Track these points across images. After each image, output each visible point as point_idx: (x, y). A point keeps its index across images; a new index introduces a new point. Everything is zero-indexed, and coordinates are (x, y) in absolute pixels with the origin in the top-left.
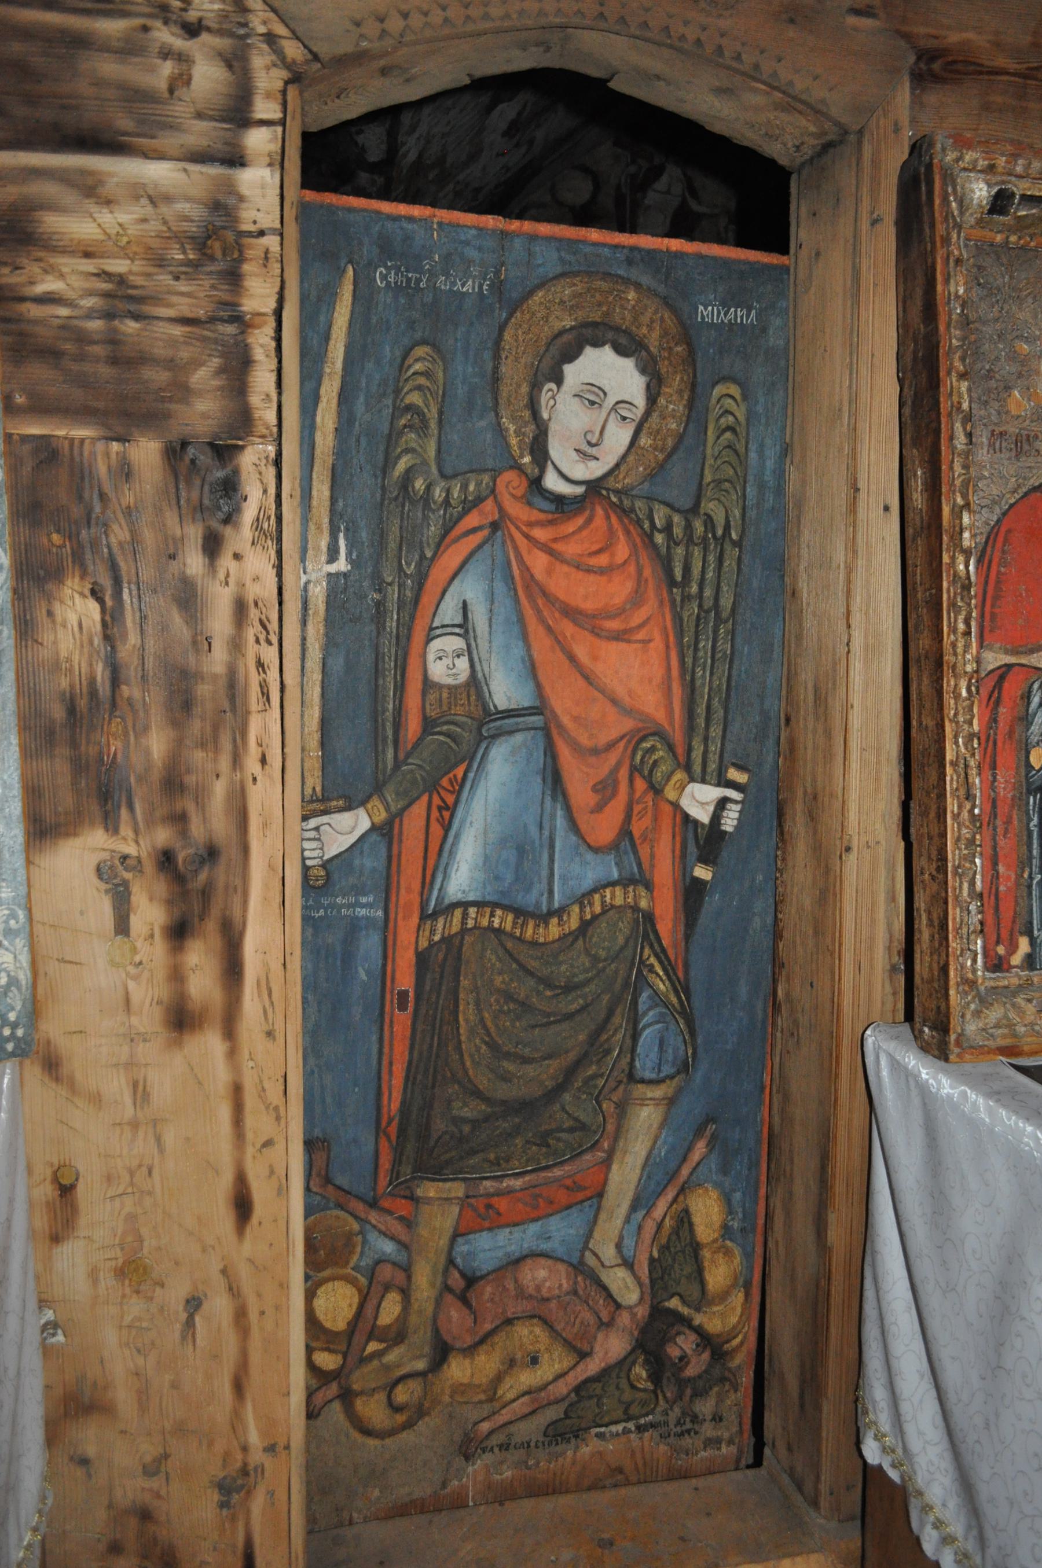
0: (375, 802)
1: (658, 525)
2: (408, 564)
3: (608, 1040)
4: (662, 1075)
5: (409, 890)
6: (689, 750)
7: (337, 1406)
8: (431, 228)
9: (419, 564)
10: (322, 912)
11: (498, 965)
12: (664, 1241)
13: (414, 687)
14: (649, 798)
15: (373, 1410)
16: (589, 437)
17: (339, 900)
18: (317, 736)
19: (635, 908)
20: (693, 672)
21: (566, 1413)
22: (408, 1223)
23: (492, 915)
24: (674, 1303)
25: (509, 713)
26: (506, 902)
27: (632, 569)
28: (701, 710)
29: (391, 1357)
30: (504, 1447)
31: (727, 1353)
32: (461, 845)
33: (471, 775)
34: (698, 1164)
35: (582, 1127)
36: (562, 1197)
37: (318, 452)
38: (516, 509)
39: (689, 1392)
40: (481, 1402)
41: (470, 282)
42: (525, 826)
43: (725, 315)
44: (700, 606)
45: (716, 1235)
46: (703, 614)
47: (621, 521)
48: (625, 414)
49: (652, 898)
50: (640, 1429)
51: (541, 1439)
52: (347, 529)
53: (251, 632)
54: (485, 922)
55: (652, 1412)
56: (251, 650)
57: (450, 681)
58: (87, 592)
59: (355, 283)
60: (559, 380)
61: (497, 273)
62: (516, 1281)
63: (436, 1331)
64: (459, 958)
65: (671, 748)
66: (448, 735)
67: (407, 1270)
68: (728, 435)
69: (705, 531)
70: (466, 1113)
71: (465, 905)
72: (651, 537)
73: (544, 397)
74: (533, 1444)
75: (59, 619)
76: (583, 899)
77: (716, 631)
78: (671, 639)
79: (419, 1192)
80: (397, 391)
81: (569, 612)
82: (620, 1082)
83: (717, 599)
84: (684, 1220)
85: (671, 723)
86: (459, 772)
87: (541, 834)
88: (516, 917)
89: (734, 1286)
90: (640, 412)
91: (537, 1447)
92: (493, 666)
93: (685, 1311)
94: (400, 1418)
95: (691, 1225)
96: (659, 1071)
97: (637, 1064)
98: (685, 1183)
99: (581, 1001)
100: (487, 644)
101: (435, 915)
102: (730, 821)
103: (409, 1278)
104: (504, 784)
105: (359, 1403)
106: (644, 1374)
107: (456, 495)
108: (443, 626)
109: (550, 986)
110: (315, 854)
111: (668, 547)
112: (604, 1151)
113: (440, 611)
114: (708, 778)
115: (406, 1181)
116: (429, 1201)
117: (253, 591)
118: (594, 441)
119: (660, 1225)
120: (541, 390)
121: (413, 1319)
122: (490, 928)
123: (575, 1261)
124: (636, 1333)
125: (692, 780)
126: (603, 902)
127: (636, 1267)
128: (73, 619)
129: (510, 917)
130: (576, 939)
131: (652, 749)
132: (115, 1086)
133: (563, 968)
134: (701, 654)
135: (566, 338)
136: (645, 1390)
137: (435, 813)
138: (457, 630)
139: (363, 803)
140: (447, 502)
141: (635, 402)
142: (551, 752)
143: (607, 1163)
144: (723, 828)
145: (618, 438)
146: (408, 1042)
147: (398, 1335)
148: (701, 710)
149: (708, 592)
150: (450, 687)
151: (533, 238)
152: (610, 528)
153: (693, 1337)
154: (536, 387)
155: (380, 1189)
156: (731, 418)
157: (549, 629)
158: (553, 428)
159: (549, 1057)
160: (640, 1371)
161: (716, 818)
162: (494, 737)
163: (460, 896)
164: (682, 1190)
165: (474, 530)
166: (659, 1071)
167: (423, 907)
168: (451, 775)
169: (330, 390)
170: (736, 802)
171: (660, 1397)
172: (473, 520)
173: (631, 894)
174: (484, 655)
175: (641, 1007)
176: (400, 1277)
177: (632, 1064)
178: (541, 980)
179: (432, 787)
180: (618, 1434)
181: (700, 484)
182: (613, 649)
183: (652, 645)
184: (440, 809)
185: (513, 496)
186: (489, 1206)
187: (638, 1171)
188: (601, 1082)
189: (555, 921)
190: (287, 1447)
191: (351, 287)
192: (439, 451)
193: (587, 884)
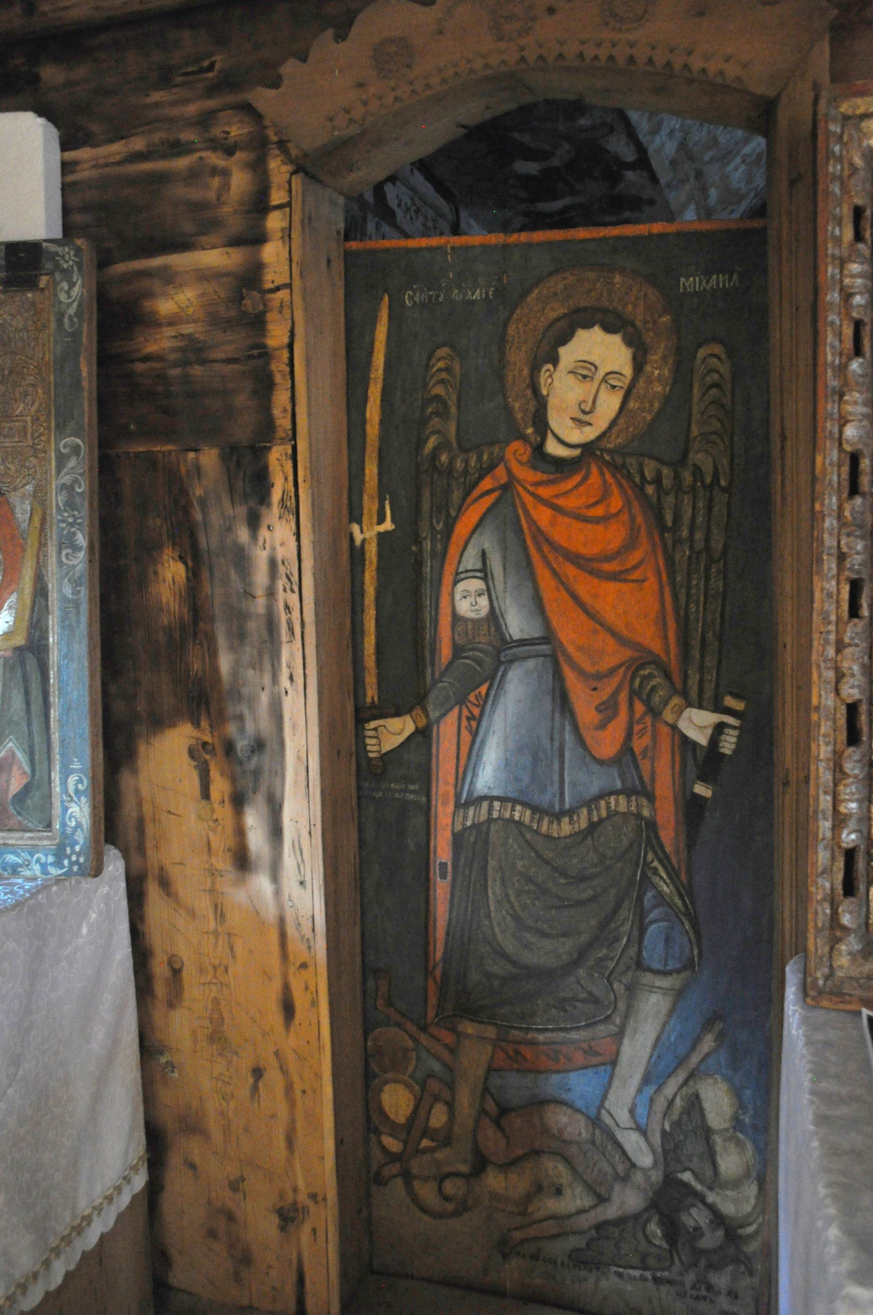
0: (418, 711)
1: (649, 479)
2: (438, 523)
3: (616, 929)
4: (668, 968)
5: (446, 783)
6: (686, 678)
7: (399, 1183)
8: (446, 254)
9: (445, 524)
10: (381, 794)
11: (519, 851)
12: (675, 1117)
13: (445, 622)
14: (648, 720)
15: (427, 1192)
16: (583, 407)
17: (393, 785)
18: (373, 658)
19: (638, 816)
20: (687, 606)
21: (588, 1244)
22: (452, 1051)
23: (513, 810)
24: (687, 1176)
25: (522, 642)
26: (525, 799)
27: (625, 517)
28: (696, 642)
29: (440, 1155)
30: (535, 1257)
31: (740, 1237)
32: (486, 750)
33: (493, 692)
34: (708, 1055)
35: (594, 1000)
36: (579, 1058)
37: (368, 440)
38: (526, 474)
39: (703, 1262)
40: (510, 1213)
41: (478, 291)
42: (538, 737)
43: (707, 283)
44: (691, 548)
45: (727, 1125)
46: (694, 556)
47: (614, 476)
48: (614, 383)
49: (654, 809)
50: (655, 1279)
51: (566, 1260)
52: (391, 499)
54: (507, 815)
55: (668, 1268)
56: (281, 596)
57: (473, 615)
58: (177, 558)
59: (390, 308)
60: (555, 360)
61: (500, 280)
62: (541, 1118)
63: (476, 1144)
64: (486, 841)
65: (667, 675)
66: (473, 659)
67: (451, 1087)
68: (714, 391)
69: (695, 480)
70: (495, 969)
71: (491, 799)
72: (642, 489)
73: (543, 376)
74: (559, 1261)
75: (161, 577)
76: (591, 802)
77: (707, 570)
78: (665, 578)
79: (460, 1028)
80: (425, 386)
82: (628, 968)
83: (707, 540)
84: (695, 1103)
85: (668, 653)
86: (483, 689)
87: (552, 745)
88: (533, 813)
89: (747, 1175)
90: (627, 381)
91: (562, 1265)
92: (508, 603)
93: (699, 1187)
94: (450, 1207)
95: (702, 1111)
96: (666, 964)
97: (644, 954)
98: (694, 1070)
99: (591, 892)
100: (502, 585)
101: (467, 804)
102: (728, 744)
103: (453, 1096)
104: (520, 701)
105: (417, 1184)
106: (659, 1232)
107: (473, 464)
108: (467, 571)
109: (564, 875)
110: (375, 748)
111: (659, 499)
112: (616, 1026)
113: (464, 559)
114: (705, 704)
115: (449, 1016)
116: (468, 1036)
117: (280, 553)
118: (588, 409)
119: (671, 1103)
120: (540, 371)
121: (457, 1130)
122: (511, 820)
123: (593, 1112)
124: (651, 1194)
125: (690, 705)
126: (608, 808)
127: (649, 1134)
128: (169, 576)
129: (528, 813)
130: (585, 838)
131: (650, 676)
132: (204, 904)
133: (574, 861)
134: (693, 591)
135: (559, 325)
136: (660, 1247)
137: (464, 723)
138: (478, 574)
139: (409, 711)
140: (465, 472)
141: (624, 372)
142: (558, 675)
143: (619, 1036)
144: (722, 750)
145: (609, 405)
146: (448, 905)
147: (446, 1139)
148: (696, 642)
149: (699, 535)
150: (472, 620)
151: (529, 245)
152: (605, 482)
153: (706, 1212)
154: (535, 369)
155: (429, 1021)
156: (716, 376)
157: (555, 573)
158: (551, 401)
159: (565, 935)
160: (654, 1229)
161: (714, 741)
162: (511, 662)
163: (486, 791)
164: (691, 1076)
165: (488, 492)
166: (666, 964)
167: (458, 796)
168: (477, 691)
169: (375, 392)
170: (734, 728)
171: (676, 1259)
172: (487, 484)
173: (634, 804)
174: (500, 596)
175: (647, 903)
176: (446, 1094)
177: (639, 952)
178: (555, 869)
179: (462, 701)
180: (635, 1279)
181: (687, 437)
182: (612, 587)
183: (646, 584)
184: (468, 718)
185: (520, 462)
186: (517, 1052)
187: (648, 1050)
188: (611, 965)
189: (566, 820)
190: (325, 1199)
191: (387, 310)
192: (458, 430)
193: (594, 790)
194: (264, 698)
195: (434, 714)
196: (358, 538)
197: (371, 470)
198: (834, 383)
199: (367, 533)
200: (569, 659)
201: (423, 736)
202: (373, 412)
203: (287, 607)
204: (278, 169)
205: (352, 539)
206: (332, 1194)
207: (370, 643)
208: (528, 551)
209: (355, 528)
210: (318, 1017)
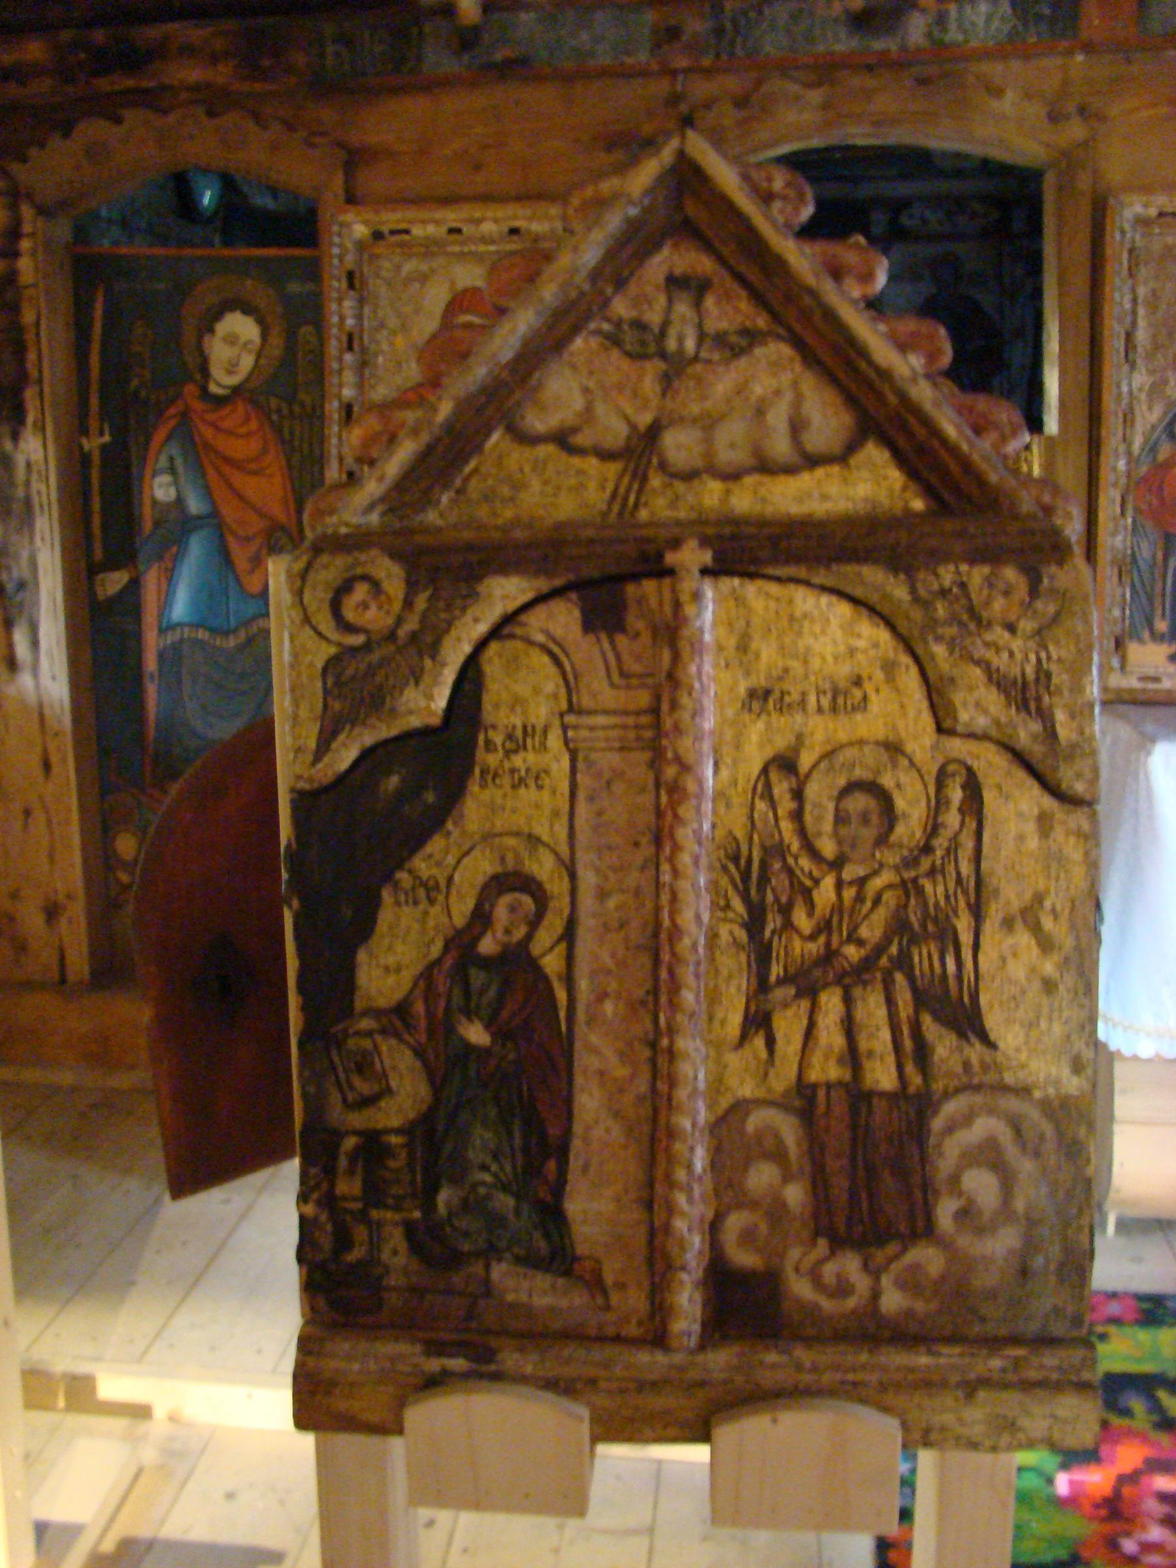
13: (147, 501)
25: (199, 518)
38: (198, 405)
53: (34, 477)
60: (212, 331)
71: (181, 625)
81: (228, 460)
117: (33, 458)
142: (222, 536)
145: (247, 362)
169: (96, 347)
172: (172, 411)
179: (161, 558)
194: (25, 554)
195: (141, 568)
196: (87, 448)
197: (94, 402)
198: (335, 366)
199: (92, 444)
200: (230, 529)
201: (135, 584)
202: (95, 361)
203: (39, 493)
204: (27, 211)
205: (81, 448)
206: (81, 893)
207: (97, 521)
208: (199, 457)
209: (84, 441)
210: (67, 770)
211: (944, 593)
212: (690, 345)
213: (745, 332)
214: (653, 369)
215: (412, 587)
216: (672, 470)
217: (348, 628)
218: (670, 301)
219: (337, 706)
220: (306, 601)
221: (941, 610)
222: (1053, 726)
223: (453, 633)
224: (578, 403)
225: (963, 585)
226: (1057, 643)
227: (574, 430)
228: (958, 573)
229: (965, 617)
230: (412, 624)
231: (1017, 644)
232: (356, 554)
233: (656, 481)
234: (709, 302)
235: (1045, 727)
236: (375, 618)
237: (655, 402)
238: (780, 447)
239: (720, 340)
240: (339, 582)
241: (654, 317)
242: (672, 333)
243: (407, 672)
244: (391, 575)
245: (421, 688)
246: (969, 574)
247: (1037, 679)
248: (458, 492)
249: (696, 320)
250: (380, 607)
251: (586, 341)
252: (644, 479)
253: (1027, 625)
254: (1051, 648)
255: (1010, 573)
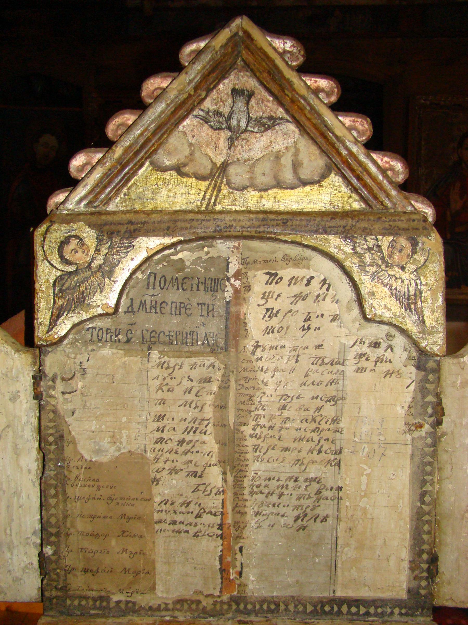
211: (369, 249)
212: (243, 124)
213: (270, 118)
214: (225, 134)
215: (99, 241)
216: (233, 185)
217: (68, 263)
218: (234, 102)
219: (60, 302)
220: (45, 249)
221: (368, 258)
222: (423, 317)
223: (120, 265)
224: (187, 152)
225: (379, 246)
226: (425, 276)
227: (185, 165)
228: (377, 240)
229: (380, 262)
230: (99, 260)
231: (405, 276)
232: (72, 224)
233: (225, 191)
234: (253, 102)
235: (419, 318)
236: (81, 258)
237: (225, 152)
238: (288, 175)
239: (259, 122)
240: (62, 239)
241: (225, 110)
242: (235, 117)
243: (97, 285)
244: (89, 235)
245: (103, 294)
246: (382, 240)
247: (415, 294)
248: (125, 195)
249: (246, 111)
250: (83, 253)
251: (192, 121)
252: (219, 191)
253: (411, 267)
254: (422, 278)
255: (403, 241)
